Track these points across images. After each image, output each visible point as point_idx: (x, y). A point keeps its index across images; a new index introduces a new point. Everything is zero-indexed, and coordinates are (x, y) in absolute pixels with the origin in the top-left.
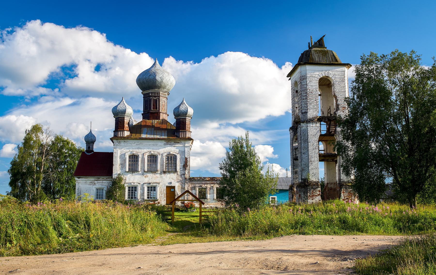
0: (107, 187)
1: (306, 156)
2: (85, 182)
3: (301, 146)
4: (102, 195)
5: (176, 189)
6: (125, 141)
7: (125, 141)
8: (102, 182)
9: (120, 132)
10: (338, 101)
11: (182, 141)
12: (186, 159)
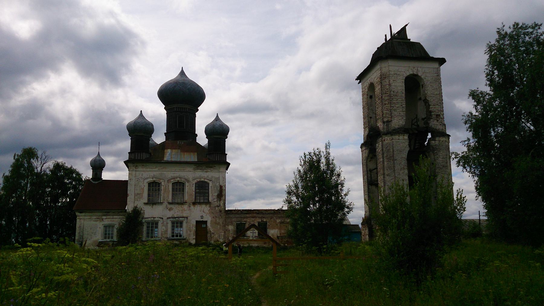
0: (119, 224)
1: (391, 178)
2: (89, 217)
3: (384, 166)
4: (112, 234)
5: (209, 224)
6: (143, 165)
7: (144, 164)
8: (112, 217)
9: (137, 154)
10: (431, 106)
11: (215, 166)
12: (221, 187)
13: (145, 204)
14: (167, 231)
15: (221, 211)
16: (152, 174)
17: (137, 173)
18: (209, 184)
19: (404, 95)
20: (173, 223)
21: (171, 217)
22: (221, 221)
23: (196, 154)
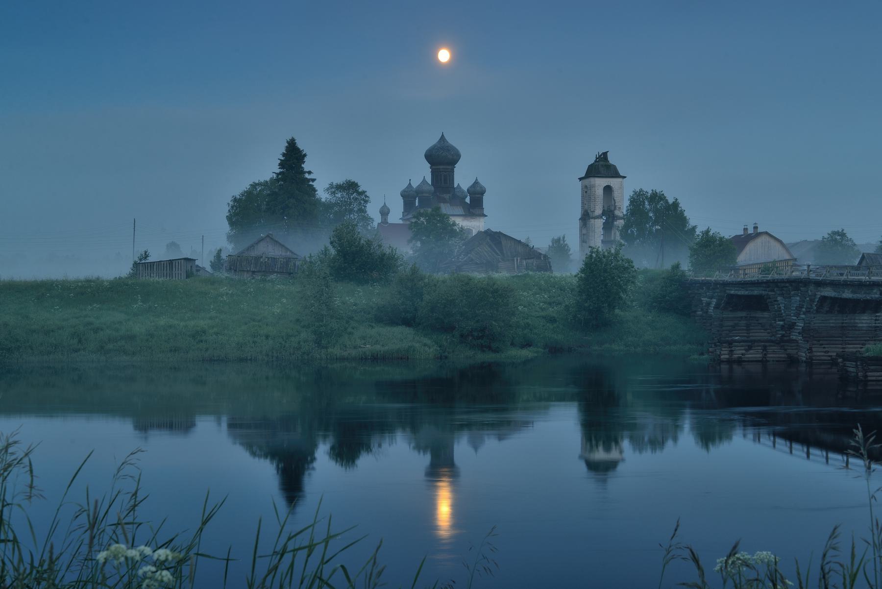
18: (472, 230)
19: (602, 197)
23: (461, 207)
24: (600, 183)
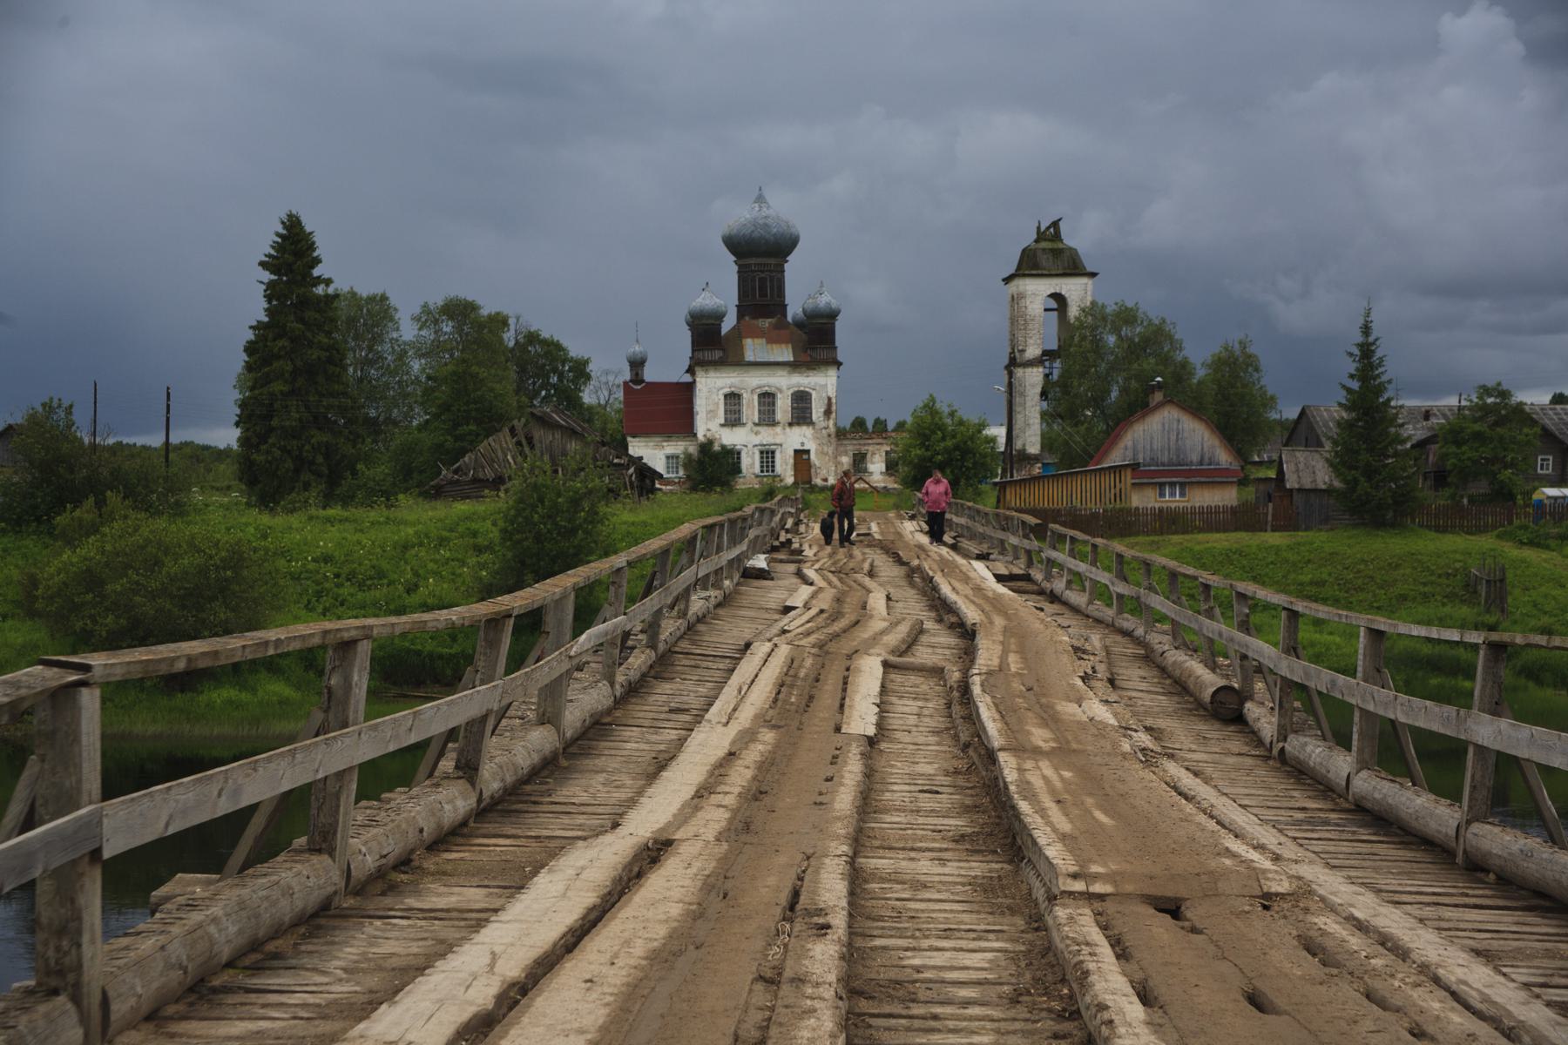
13: (722, 425)
14: (753, 464)
15: (829, 435)
16: (729, 381)
17: (709, 380)
18: (810, 395)
20: (762, 452)
21: (757, 443)
22: (830, 450)
23: (790, 346)
24: (1037, 291)
